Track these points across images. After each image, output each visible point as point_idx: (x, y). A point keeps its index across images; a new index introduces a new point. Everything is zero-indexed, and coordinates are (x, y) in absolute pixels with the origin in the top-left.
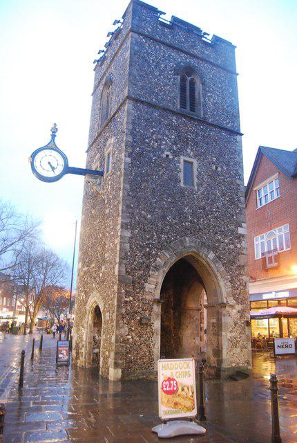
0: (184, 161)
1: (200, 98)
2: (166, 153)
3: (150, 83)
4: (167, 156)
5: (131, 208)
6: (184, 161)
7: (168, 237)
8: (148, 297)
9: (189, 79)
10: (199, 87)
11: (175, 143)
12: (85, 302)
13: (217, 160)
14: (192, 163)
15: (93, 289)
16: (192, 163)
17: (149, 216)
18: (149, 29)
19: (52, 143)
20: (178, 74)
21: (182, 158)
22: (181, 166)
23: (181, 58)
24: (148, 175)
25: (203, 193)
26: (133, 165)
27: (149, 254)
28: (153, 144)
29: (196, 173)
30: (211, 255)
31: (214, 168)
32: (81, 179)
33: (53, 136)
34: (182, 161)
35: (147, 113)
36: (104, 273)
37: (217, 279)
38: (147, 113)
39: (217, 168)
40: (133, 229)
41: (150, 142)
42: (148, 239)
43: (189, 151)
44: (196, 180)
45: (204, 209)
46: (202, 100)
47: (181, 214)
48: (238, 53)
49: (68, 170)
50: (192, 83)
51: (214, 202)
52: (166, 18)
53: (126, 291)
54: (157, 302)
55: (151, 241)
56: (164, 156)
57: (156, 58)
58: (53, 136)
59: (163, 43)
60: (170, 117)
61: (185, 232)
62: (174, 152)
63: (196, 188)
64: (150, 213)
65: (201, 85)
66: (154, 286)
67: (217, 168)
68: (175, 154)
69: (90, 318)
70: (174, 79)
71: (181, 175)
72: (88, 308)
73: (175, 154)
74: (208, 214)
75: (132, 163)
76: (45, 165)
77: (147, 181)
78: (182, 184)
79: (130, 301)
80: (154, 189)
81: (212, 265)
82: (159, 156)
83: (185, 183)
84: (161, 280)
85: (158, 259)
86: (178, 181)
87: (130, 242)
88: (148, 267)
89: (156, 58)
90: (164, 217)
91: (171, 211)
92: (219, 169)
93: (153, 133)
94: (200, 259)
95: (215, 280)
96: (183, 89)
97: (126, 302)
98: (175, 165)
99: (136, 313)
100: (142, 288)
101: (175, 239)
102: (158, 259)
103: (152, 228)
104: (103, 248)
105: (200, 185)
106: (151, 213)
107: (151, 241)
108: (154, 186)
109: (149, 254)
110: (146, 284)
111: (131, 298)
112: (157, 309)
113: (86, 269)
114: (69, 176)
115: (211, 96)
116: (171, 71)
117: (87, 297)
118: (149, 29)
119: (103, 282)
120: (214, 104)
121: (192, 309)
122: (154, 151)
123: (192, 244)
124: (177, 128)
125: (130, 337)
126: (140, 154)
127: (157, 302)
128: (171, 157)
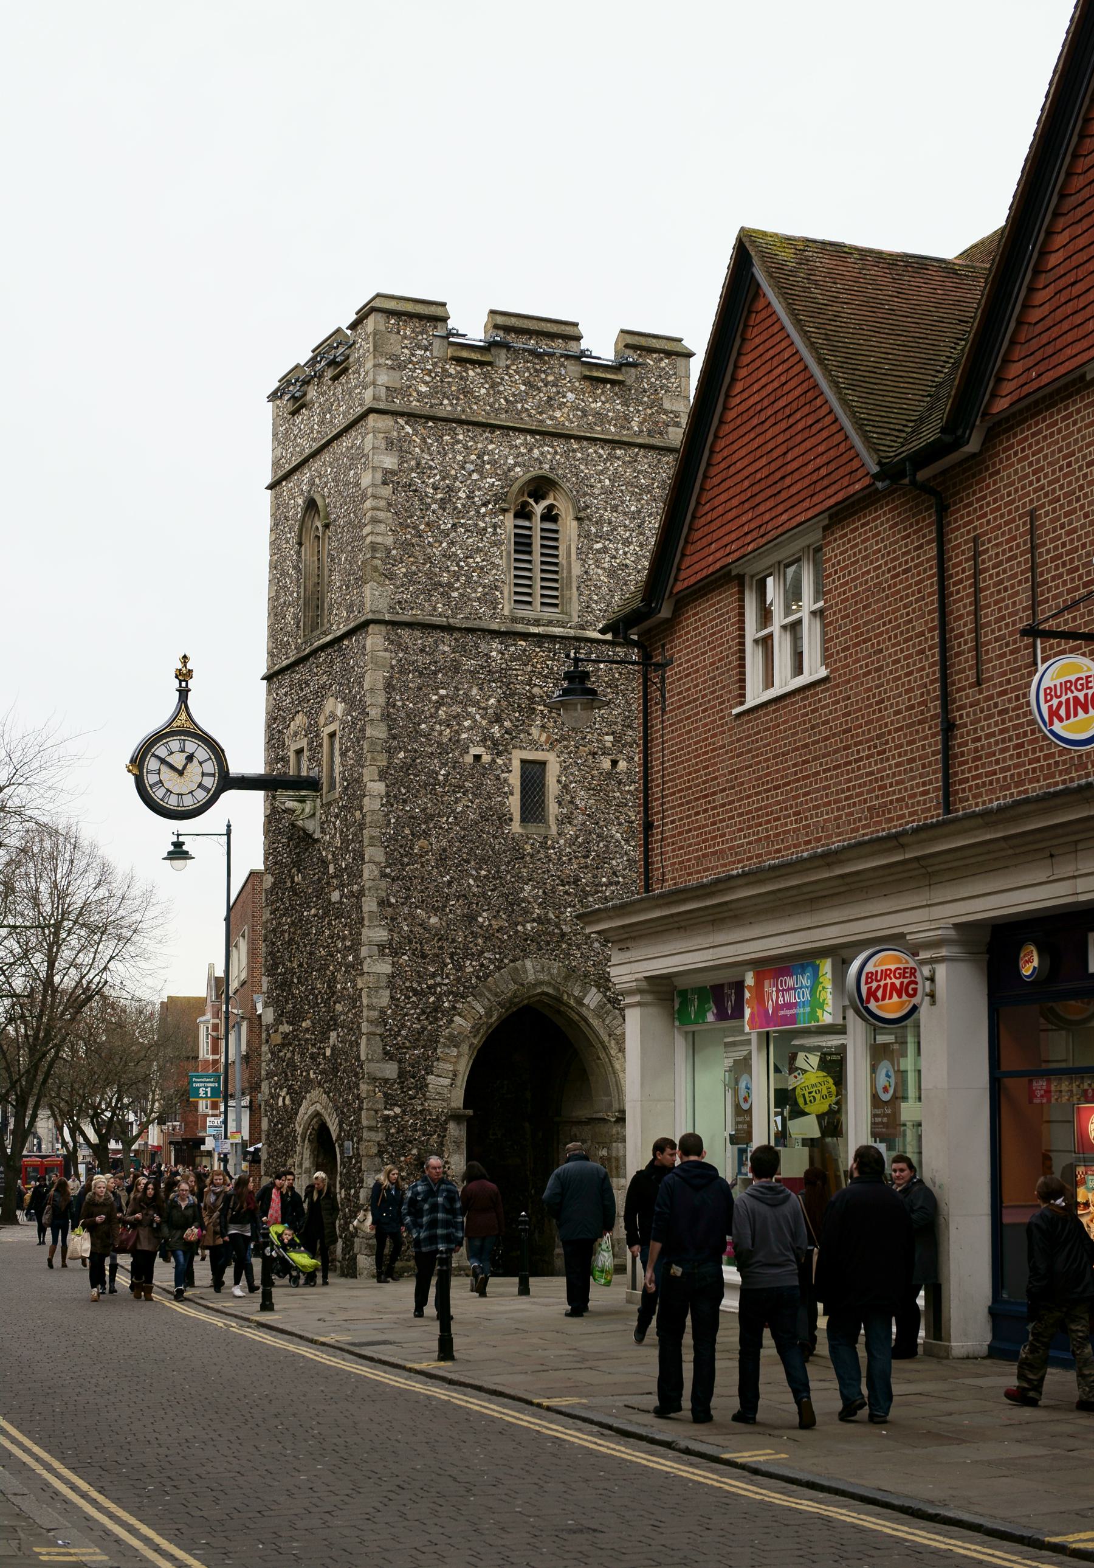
0: (523, 761)
1: (569, 564)
2: (474, 750)
3: (429, 559)
4: (477, 758)
5: (390, 905)
6: (523, 761)
7: (482, 965)
8: (437, 1107)
9: (539, 509)
10: (569, 527)
11: (498, 719)
12: (291, 1114)
13: (616, 741)
14: (543, 764)
15: (308, 1080)
16: (543, 764)
17: (434, 920)
18: (424, 389)
19: (184, 716)
20: (504, 511)
21: (517, 756)
22: (515, 779)
23: (519, 459)
25: (572, 843)
26: (390, 799)
27: (437, 1008)
28: (441, 733)
29: (553, 787)
31: (606, 764)
32: (257, 799)
33: (183, 693)
34: (516, 765)
35: (422, 651)
36: (333, 1049)
37: (608, 1055)
38: (422, 651)
39: (614, 763)
40: (395, 953)
41: (432, 729)
42: (433, 976)
43: (535, 731)
44: (553, 809)
45: (577, 880)
46: (577, 569)
47: (513, 904)
49: (228, 782)
50: (550, 516)
51: (602, 859)
52: (470, 325)
53: (385, 1094)
54: (455, 1117)
55: (438, 979)
56: (469, 759)
57: (443, 479)
58: (183, 693)
59: (461, 422)
60: (483, 648)
61: (524, 946)
62: (496, 744)
63: (554, 829)
64: (436, 910)
65: (575, 523)
66: (447, 1083)
67: (614, 763)
68: (498, 748)
69: (307, 1153)
70: (495, 527)
71: (514, 803)
72: (300, 1130)
73: (498, 748)
74: (587, 895)
75: (388, 795)
76: (172, 767)
77: (426, 834)
78: (516, 827)
79: (396, 1116)
80: (445, 850)
81: (595, 1022)
82: (455, 764)
83: (523, 820)
84: (464, 1067)
85: (457, 1019)
86: (505, 819)
87: (391, 985)
88: (433, 1041)
89: (443, 479)
90: (471, 918)
91: (488, 899)
92: (622, 765)
93: (439, 704)
95: (602, 1055)
96: (523, 544)
97: (386, 1119)
98: (498, 778)
99: (410, 1142)
100: (422, 1087)
101: (499, 968)
102: (457, 1019)
103: (441, 948)
104: (329, 987)
105: (565, 820)
107: (438, 979)
108: (444, 843)
109: (437, 1008)
110: (430, 1077)
111: (398, 1110)
112: (456, 1131)
113: (286, 1028)
114: (230, 796)
115: (605, 550)
116: (485, 505)
117: (297, 1102)
118: (424, 389)
119: (335, 1070)
120: (612, 573)
121: (580, 1123)
122: (443, 749)
123: (541, 977)
124: (502, 676)
126: (406, 767)
127: (455, 1117)
128: (486, 759)
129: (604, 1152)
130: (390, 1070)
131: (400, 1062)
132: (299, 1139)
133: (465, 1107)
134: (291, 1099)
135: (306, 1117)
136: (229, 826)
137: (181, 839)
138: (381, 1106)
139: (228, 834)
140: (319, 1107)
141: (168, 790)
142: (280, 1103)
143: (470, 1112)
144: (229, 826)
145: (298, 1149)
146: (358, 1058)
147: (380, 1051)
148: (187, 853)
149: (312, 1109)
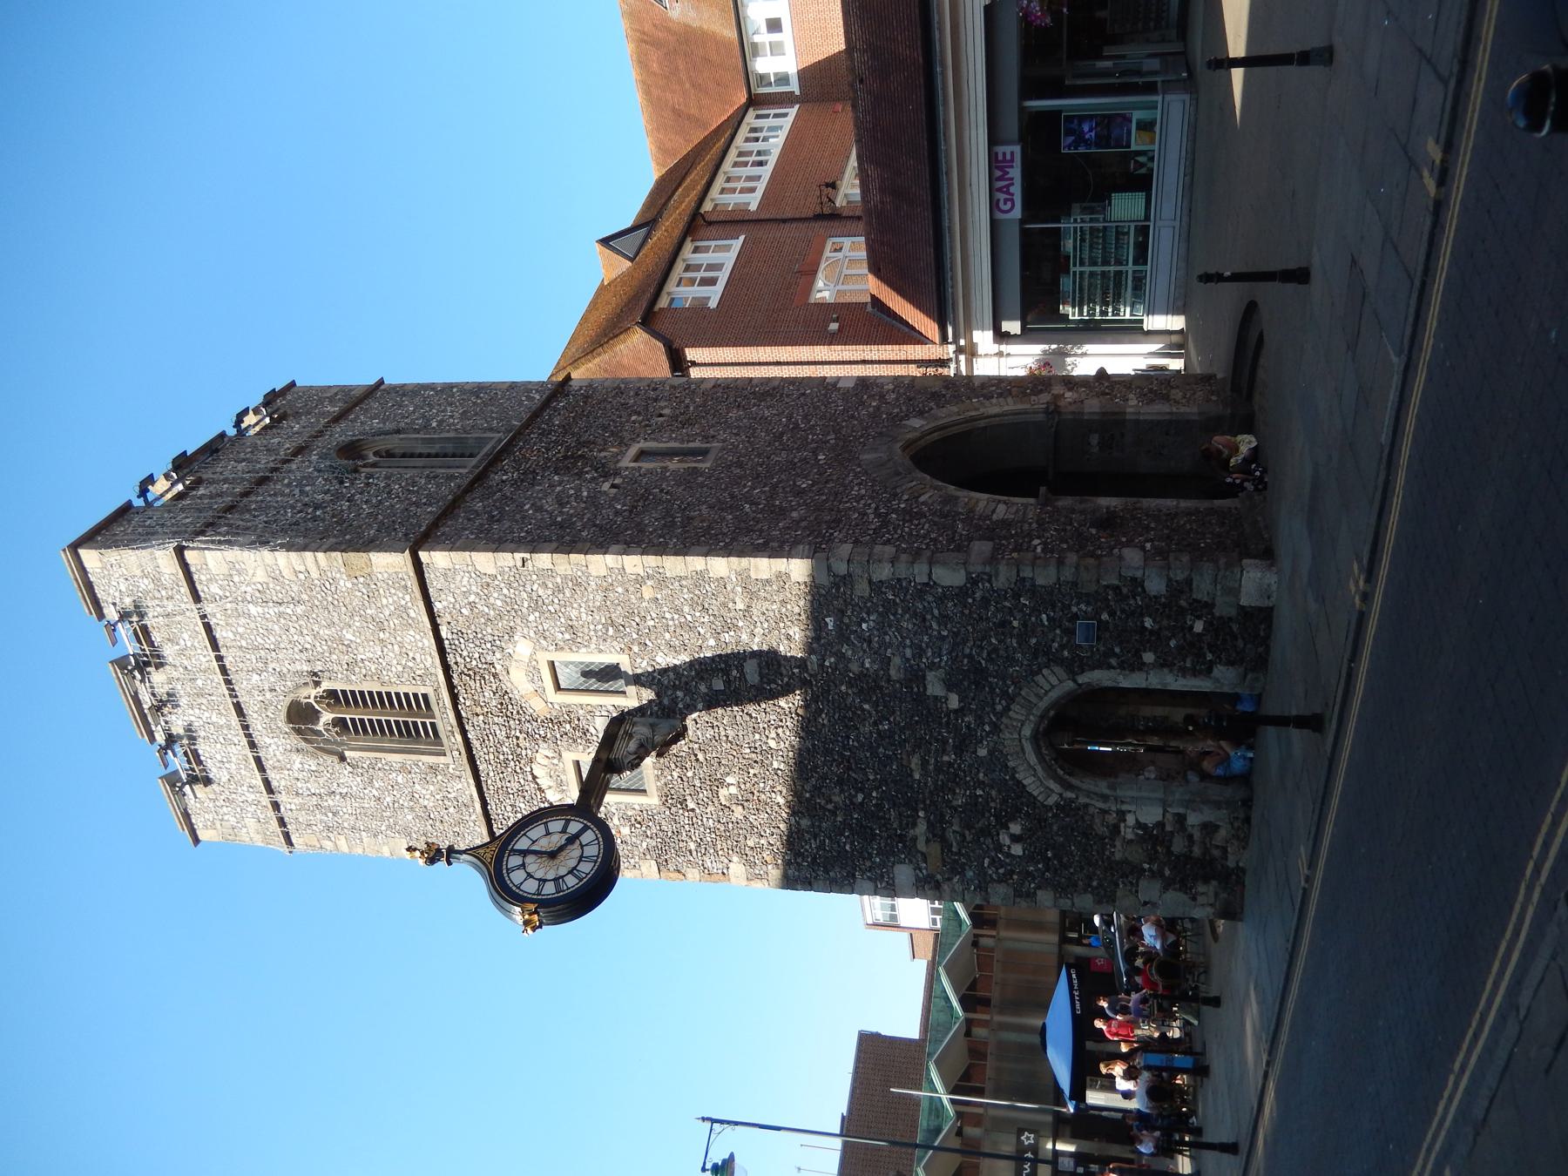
24: (668, 513)
30: (916, 423)
48: (312, 376)
53: (1014, 550)
56: (614, 491)
90: (800, 493)
94: (922, 443)
106: (783, 512)
112: (1065, 502)
117: (1016, 800)
125: (1148, 545)
129: (1094, 439)
130: (981, 548)
131: (970, 539)
132: (1069, 795)
133: (1036, 496)
134: (1013, 819)
135: (1039, 768)
136: (704, 1119)
137: (709, 1166)
138: (1030, 555)
139: (714, 1121)
140: (1027, 732)
141: (570, 872)
142: (1017, 850)
143: (1043, 490)
144: (704, 1119)
145: (1083, 800)
146: (962, 593)
147: (955, 554)
148: (724, 1161)
149: (1028, 747)
